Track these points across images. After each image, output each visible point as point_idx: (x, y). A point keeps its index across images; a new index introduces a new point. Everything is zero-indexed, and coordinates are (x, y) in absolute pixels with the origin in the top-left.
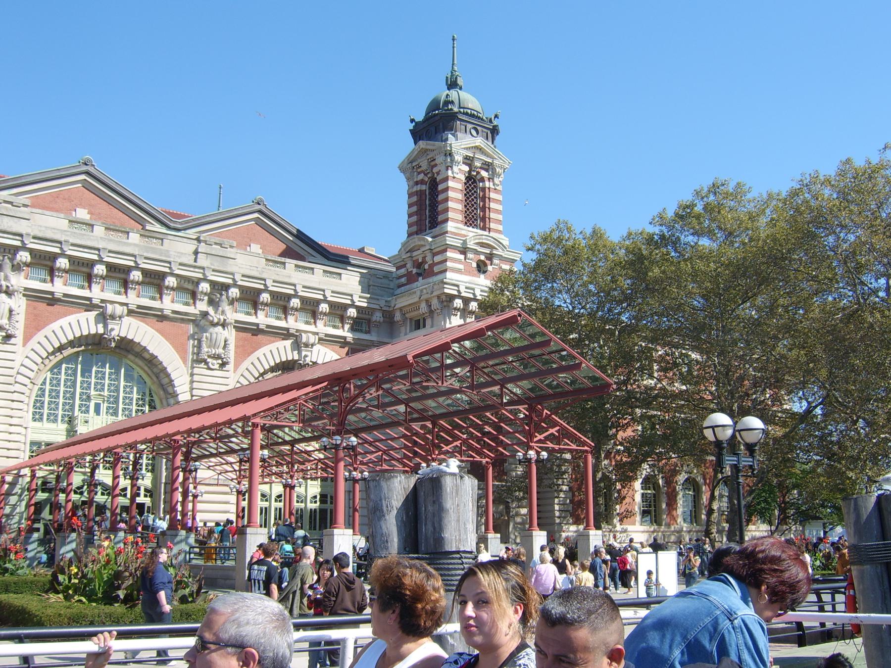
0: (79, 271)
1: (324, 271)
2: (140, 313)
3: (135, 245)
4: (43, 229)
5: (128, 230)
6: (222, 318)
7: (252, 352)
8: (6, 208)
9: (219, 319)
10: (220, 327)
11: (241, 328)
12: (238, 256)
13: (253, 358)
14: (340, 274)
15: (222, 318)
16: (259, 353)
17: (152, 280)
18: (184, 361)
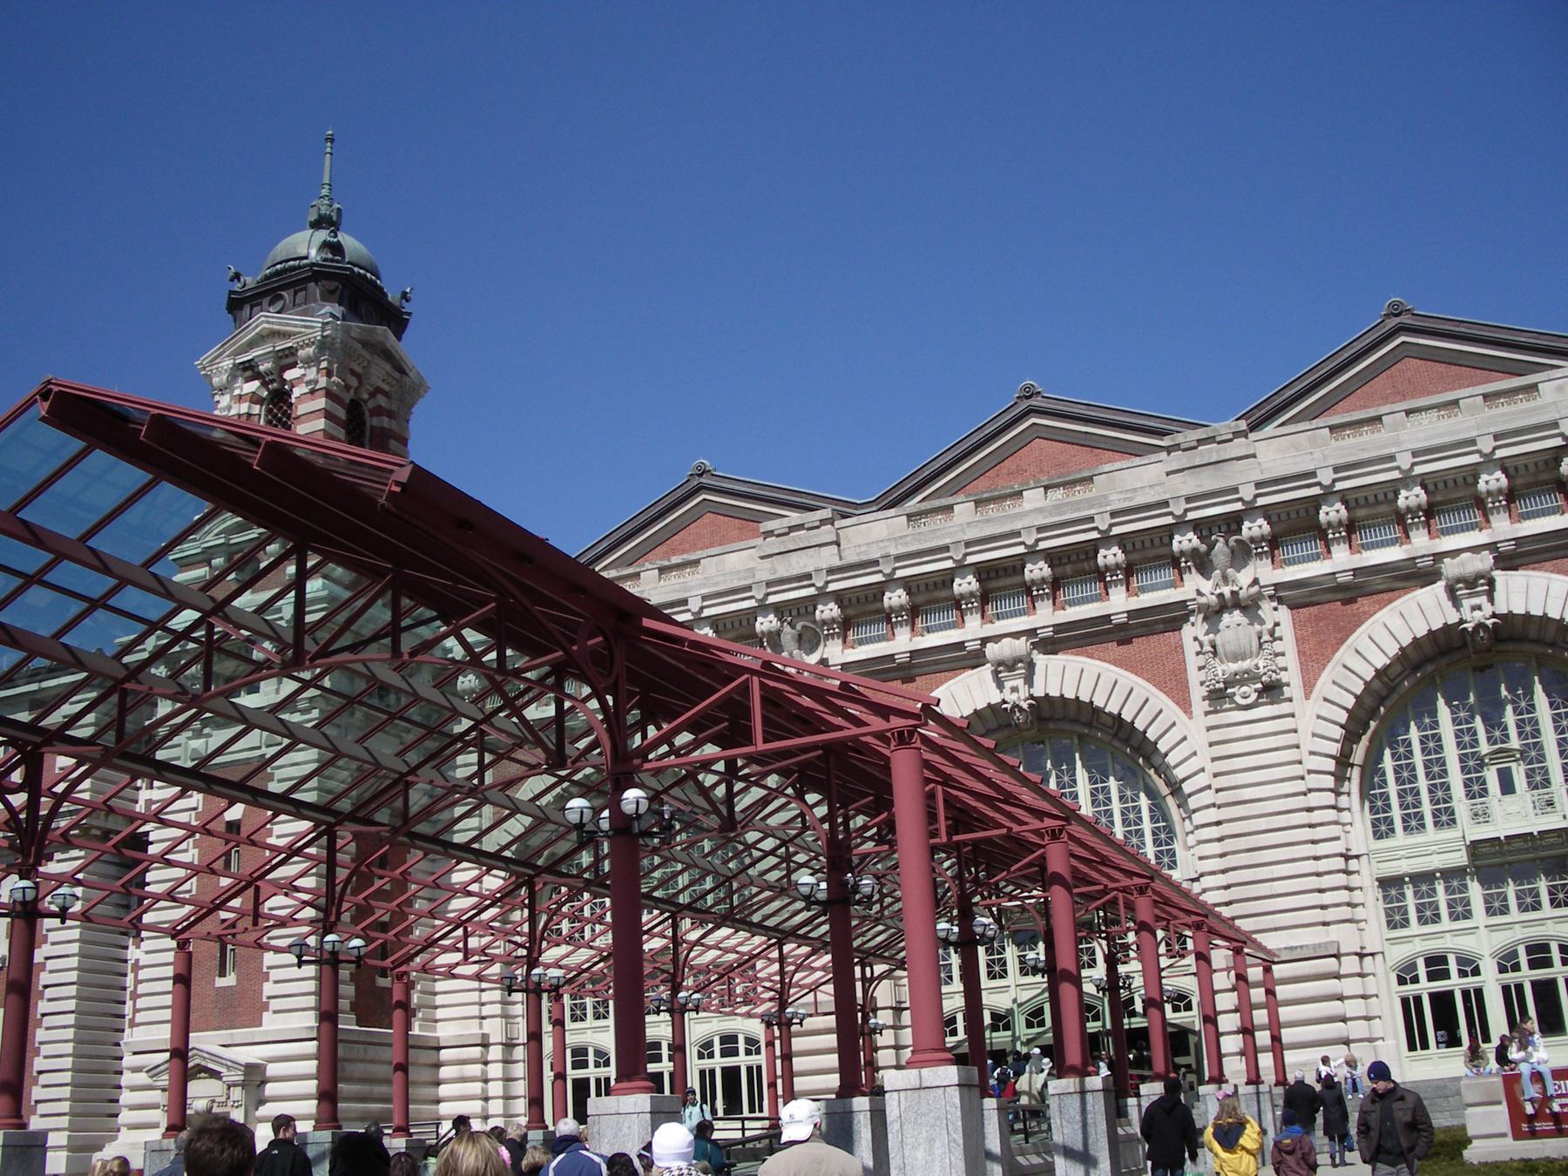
0: (937, 601)
1: (1486, 397)
2: (1058, 641)
3: (1039, 510)
4: (864, 549)
5: (1017, 488)
6: (1226, 591)
7: (1342, 641)
8: (800, 538)
9: (1221, 596)
10: (1237, 612)
11: (1295, 596)
12: (1261, 448)
13: (1344, 654)
14: (1533, 387)
15: (1226, 591)
16: (1359, 638)
17: (1079, 566)
18: (1185, 704)
